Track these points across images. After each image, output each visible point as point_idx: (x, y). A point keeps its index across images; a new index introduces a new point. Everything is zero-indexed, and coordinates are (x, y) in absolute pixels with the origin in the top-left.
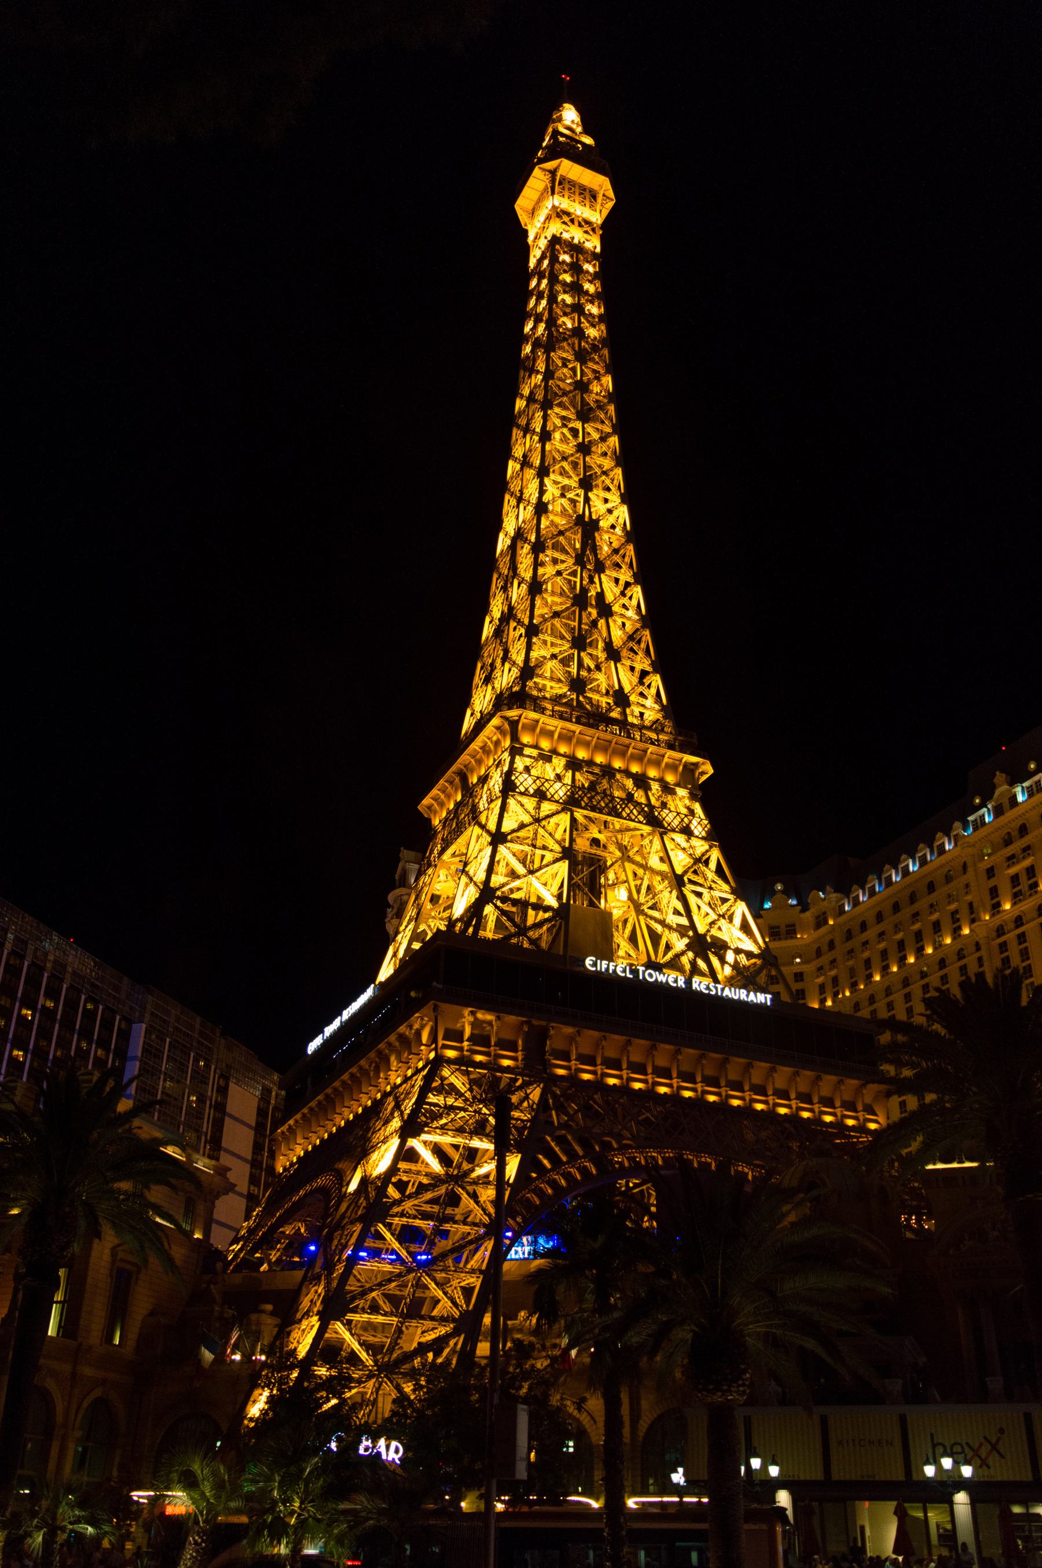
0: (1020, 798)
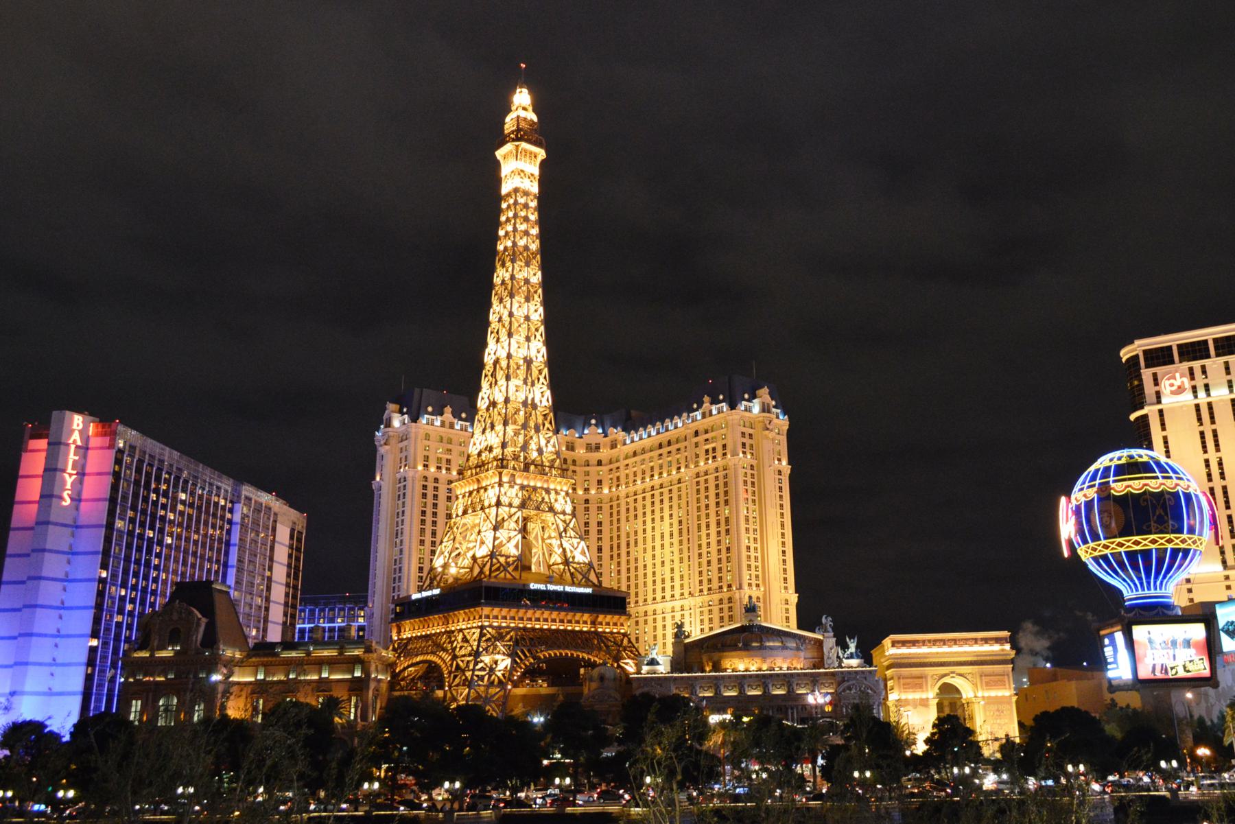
0: (714, 412)
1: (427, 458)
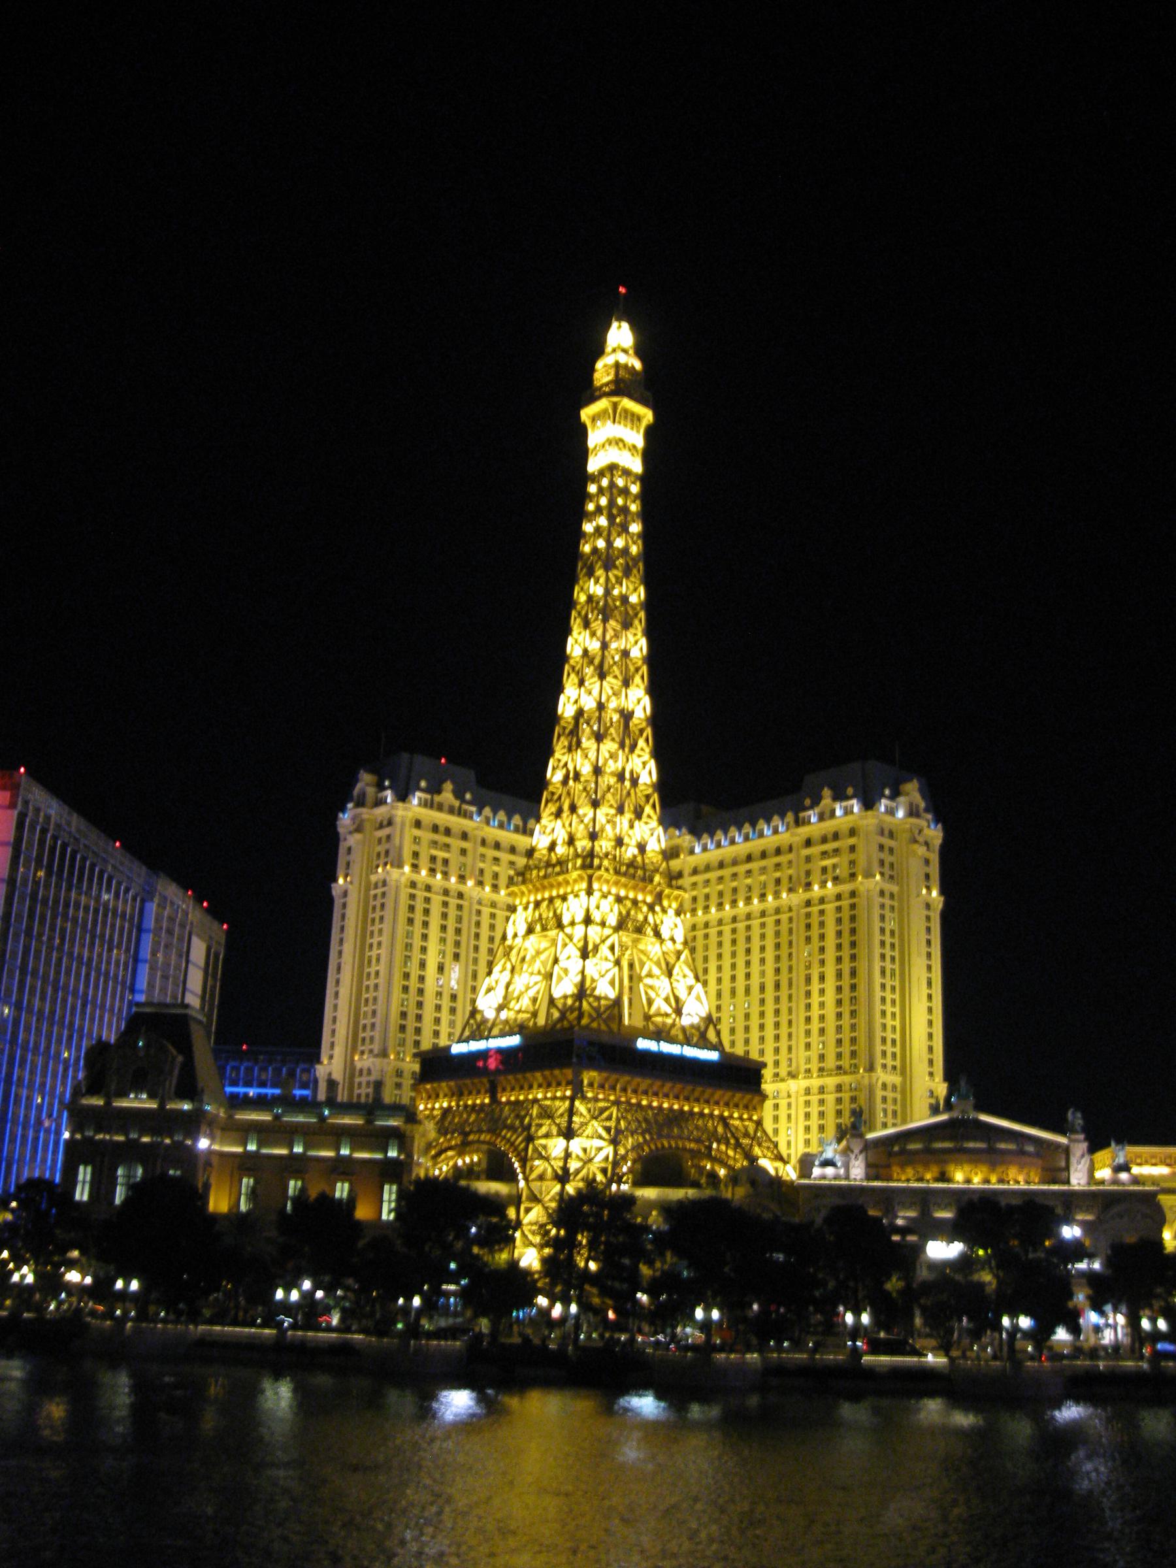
0: (839, 813)
1: (416, 855)
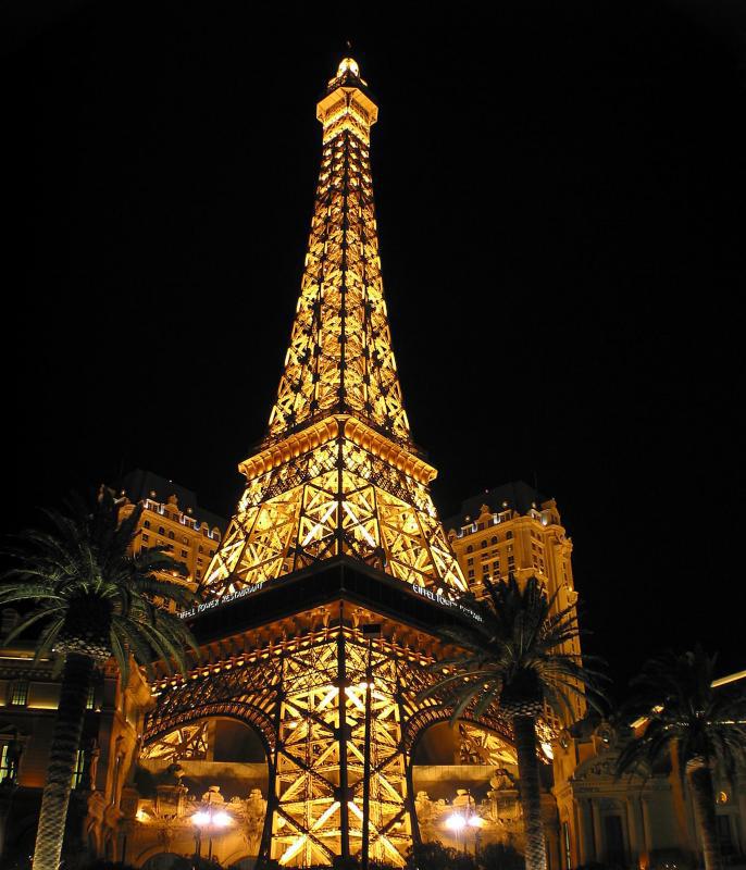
0: (496, 522)
